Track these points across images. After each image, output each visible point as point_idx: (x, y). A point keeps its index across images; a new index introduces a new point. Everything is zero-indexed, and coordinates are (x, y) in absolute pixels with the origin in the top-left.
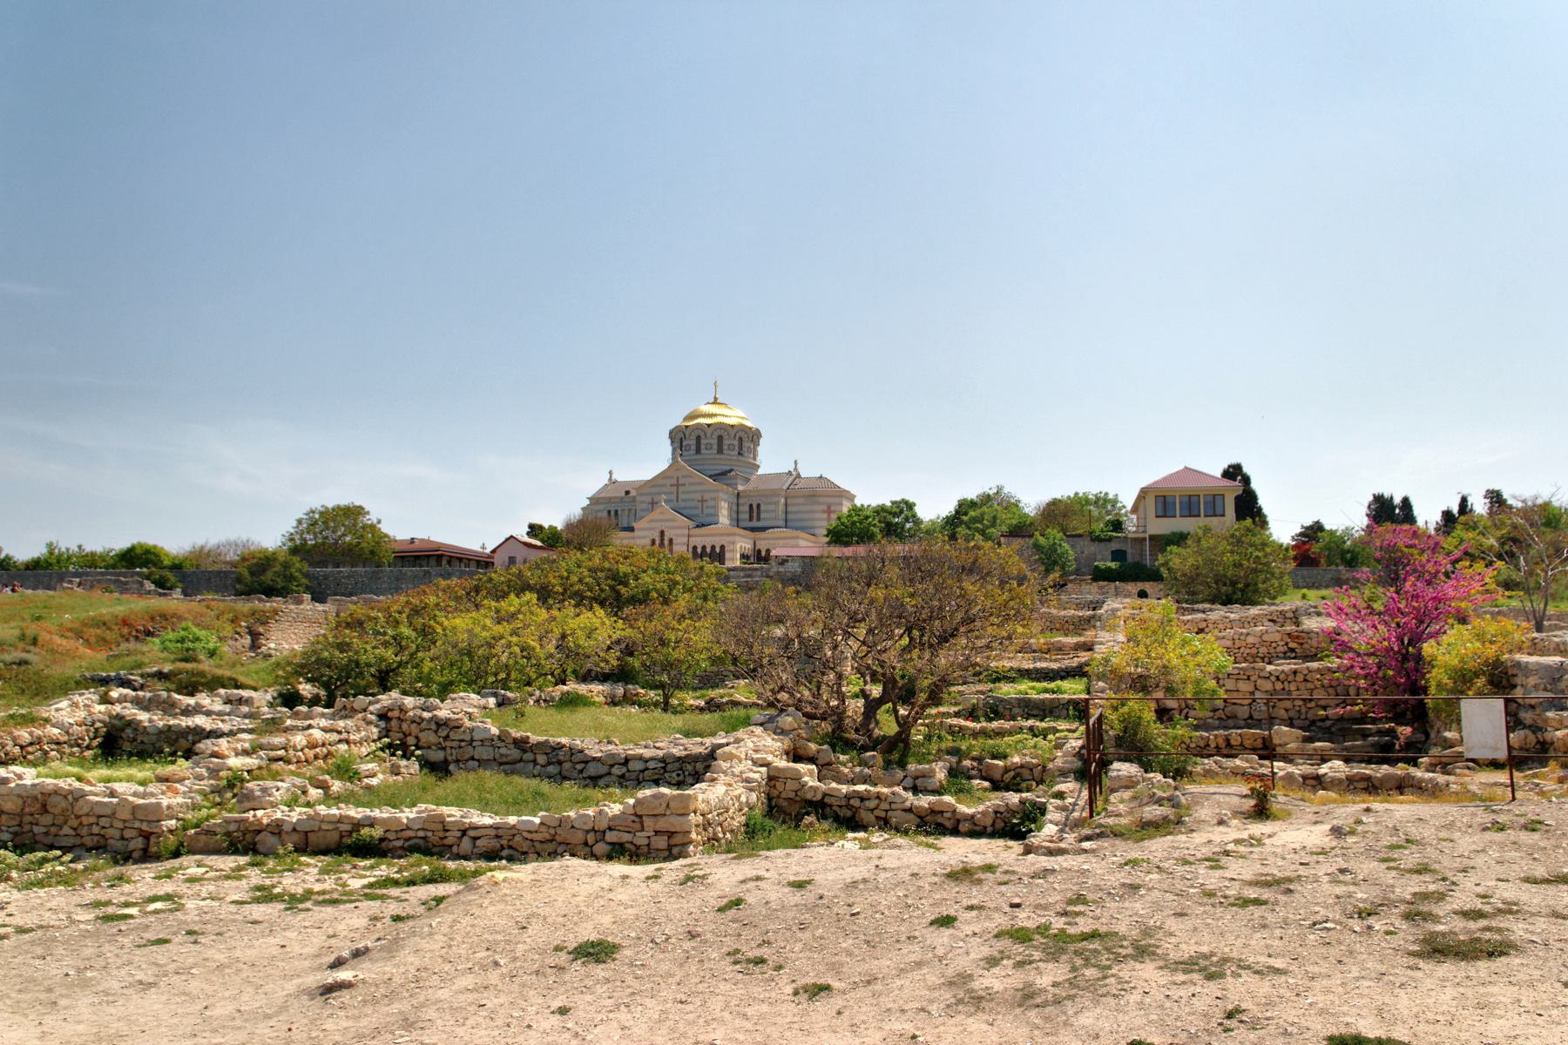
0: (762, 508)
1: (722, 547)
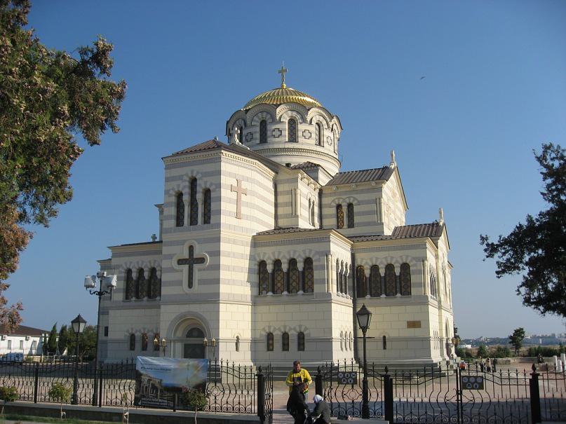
0: (356, 209)
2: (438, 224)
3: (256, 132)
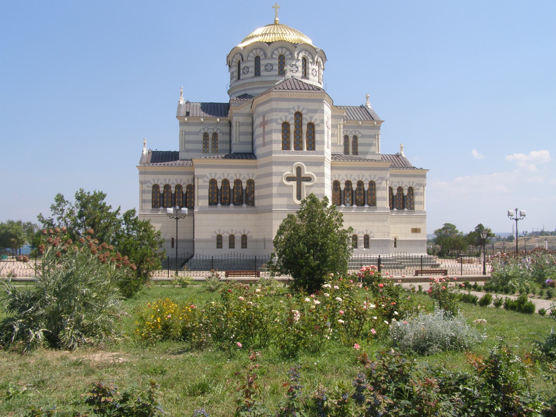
0: (360, 141)
1: (372, 184)
2: (401, 155)
3: (276, 65)
